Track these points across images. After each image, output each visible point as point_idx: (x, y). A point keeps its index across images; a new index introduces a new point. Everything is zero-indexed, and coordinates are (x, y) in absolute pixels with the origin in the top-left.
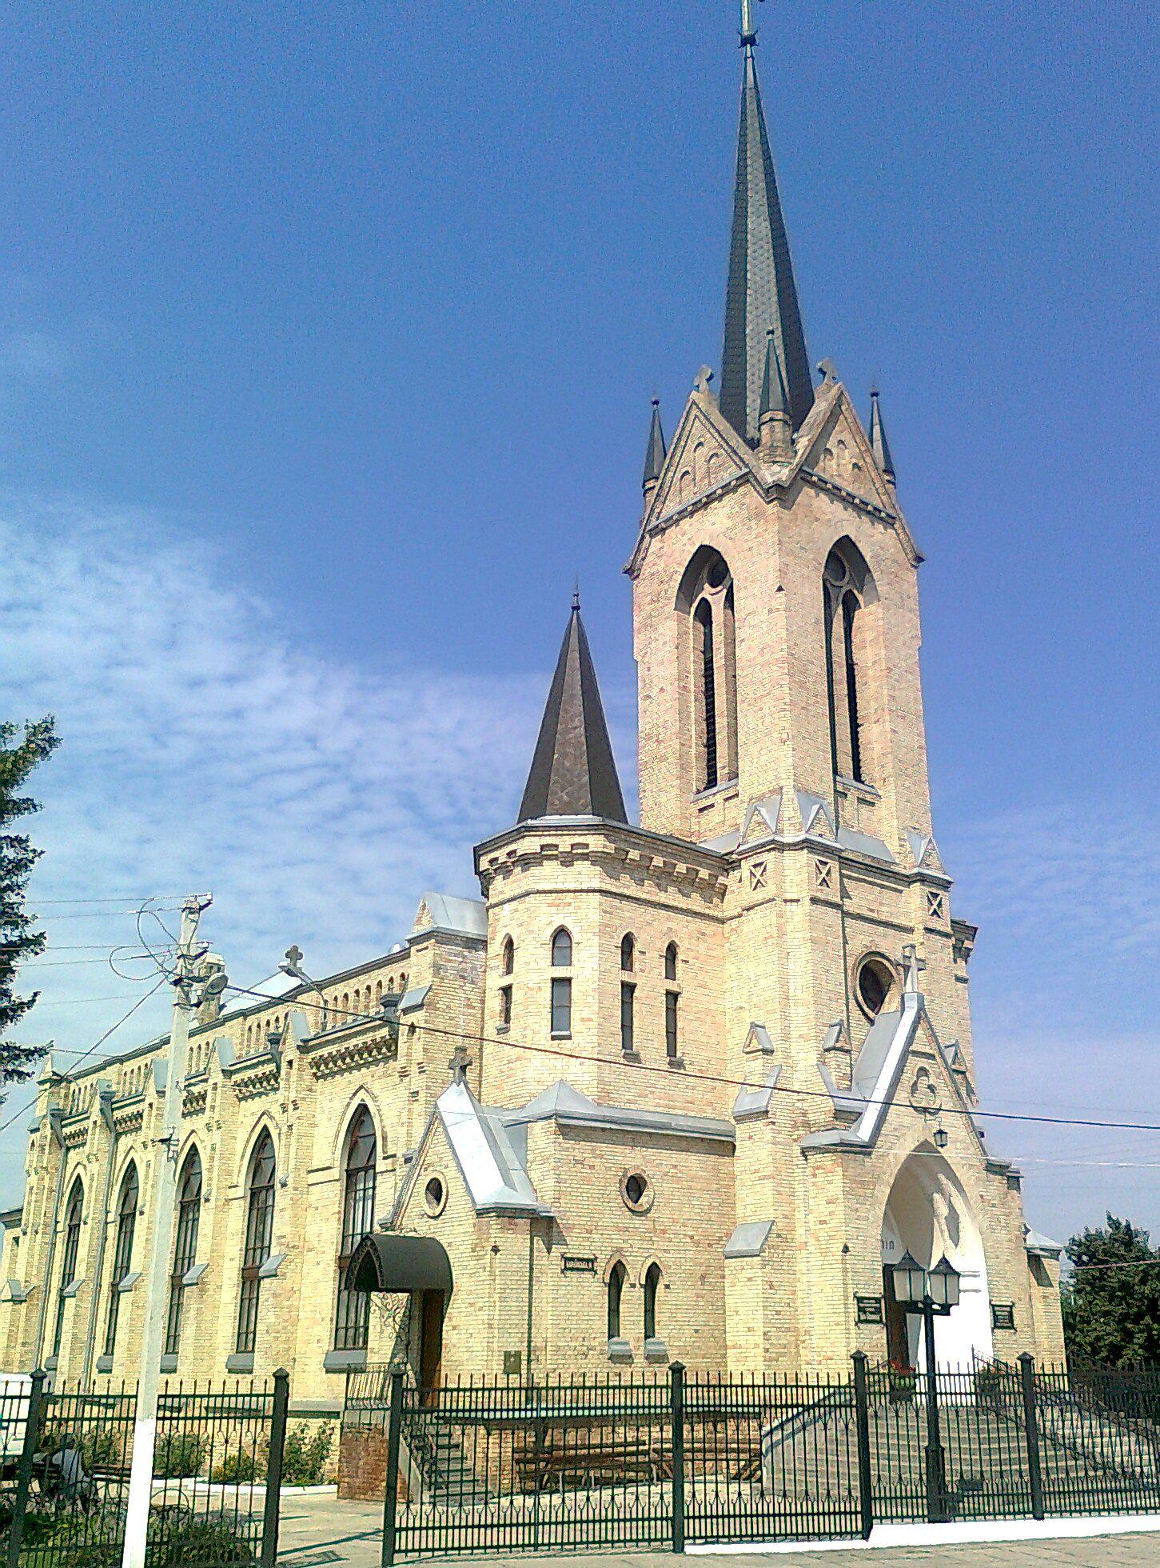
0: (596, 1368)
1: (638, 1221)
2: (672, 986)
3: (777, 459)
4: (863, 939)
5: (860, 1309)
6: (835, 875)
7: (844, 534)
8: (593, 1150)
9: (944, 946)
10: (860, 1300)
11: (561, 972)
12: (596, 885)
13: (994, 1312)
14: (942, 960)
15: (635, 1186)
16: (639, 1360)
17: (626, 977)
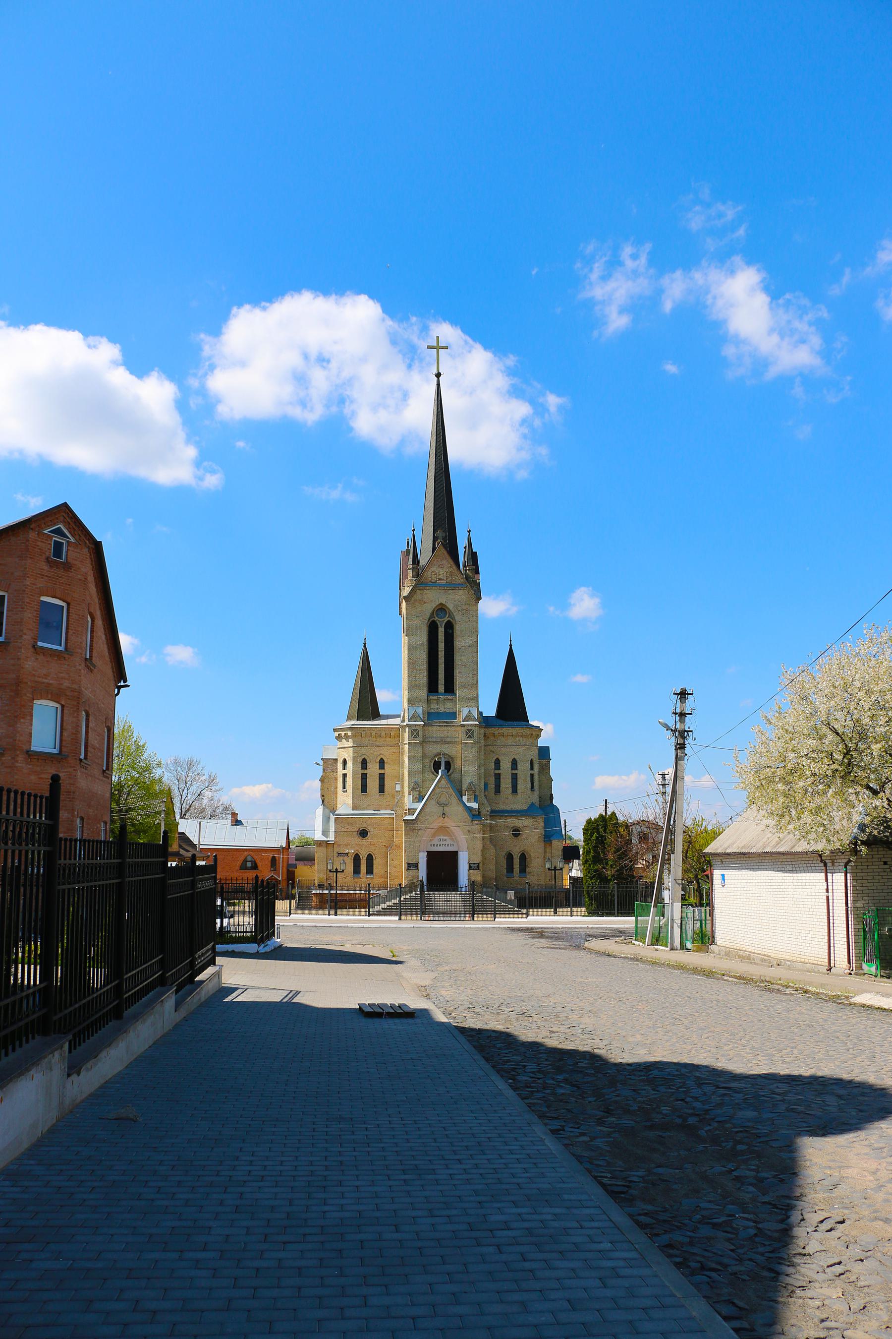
0: (349, 881)
1: (364, 842)
2: (382, 771)
3: (410, 585)
4: (433, 750)
5: (408, 866)
6: (421, 733)
7: (437, 603)
8: (348, 823)
9: (472, 748)
10: (408, 864)
11: (344, 772)
12: (352, 745)
13: (470, 865)
14: (472, 752)
15: (363, 833)
16: (364, 879)
17: (364, 771)
